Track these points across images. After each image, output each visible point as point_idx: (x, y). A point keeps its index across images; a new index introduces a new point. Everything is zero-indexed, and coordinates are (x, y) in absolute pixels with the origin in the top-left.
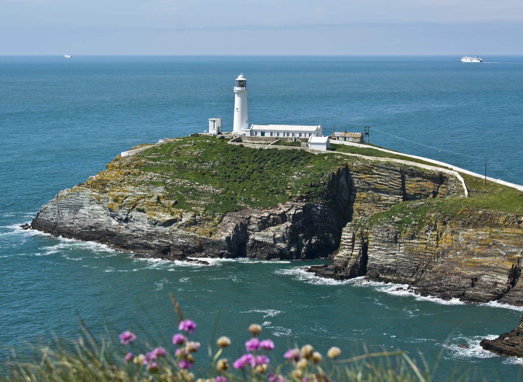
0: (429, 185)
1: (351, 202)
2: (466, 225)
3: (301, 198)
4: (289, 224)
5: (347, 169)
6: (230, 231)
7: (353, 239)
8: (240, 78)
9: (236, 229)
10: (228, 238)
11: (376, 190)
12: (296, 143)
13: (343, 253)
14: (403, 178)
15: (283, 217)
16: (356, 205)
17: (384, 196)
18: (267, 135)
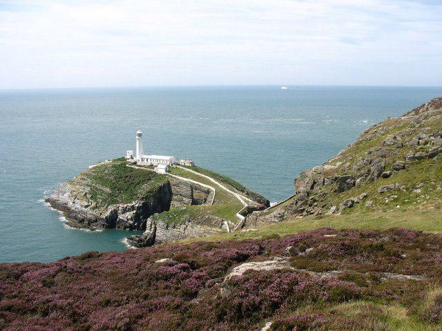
0: (203, 195)
1: (170, 200)
2: (198, 223)
3: (143, 198)
4: (135, 212)
5: (169, 183)
6: (108, 213)
7: (151, 225)
8: (139, 132)
9: (112, 212)
10: (107, 217)
11: (181, 195)
12: (152, 166)
13: (147, 231)
14: (192, 190)
15: (133, 208)
16: (172, 202)
17: (184, 199)
18: (149, 160)
